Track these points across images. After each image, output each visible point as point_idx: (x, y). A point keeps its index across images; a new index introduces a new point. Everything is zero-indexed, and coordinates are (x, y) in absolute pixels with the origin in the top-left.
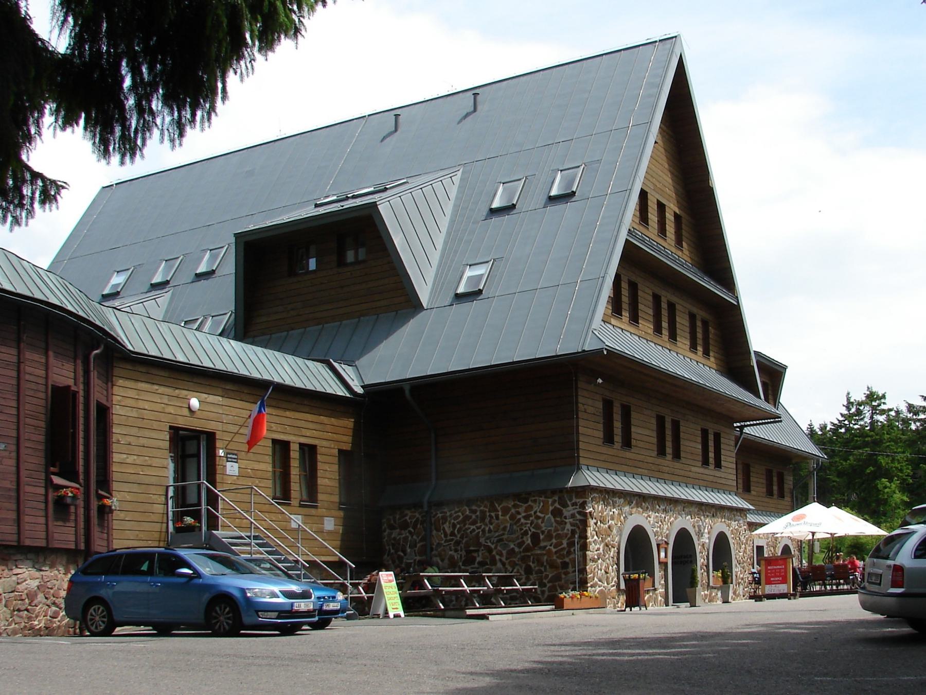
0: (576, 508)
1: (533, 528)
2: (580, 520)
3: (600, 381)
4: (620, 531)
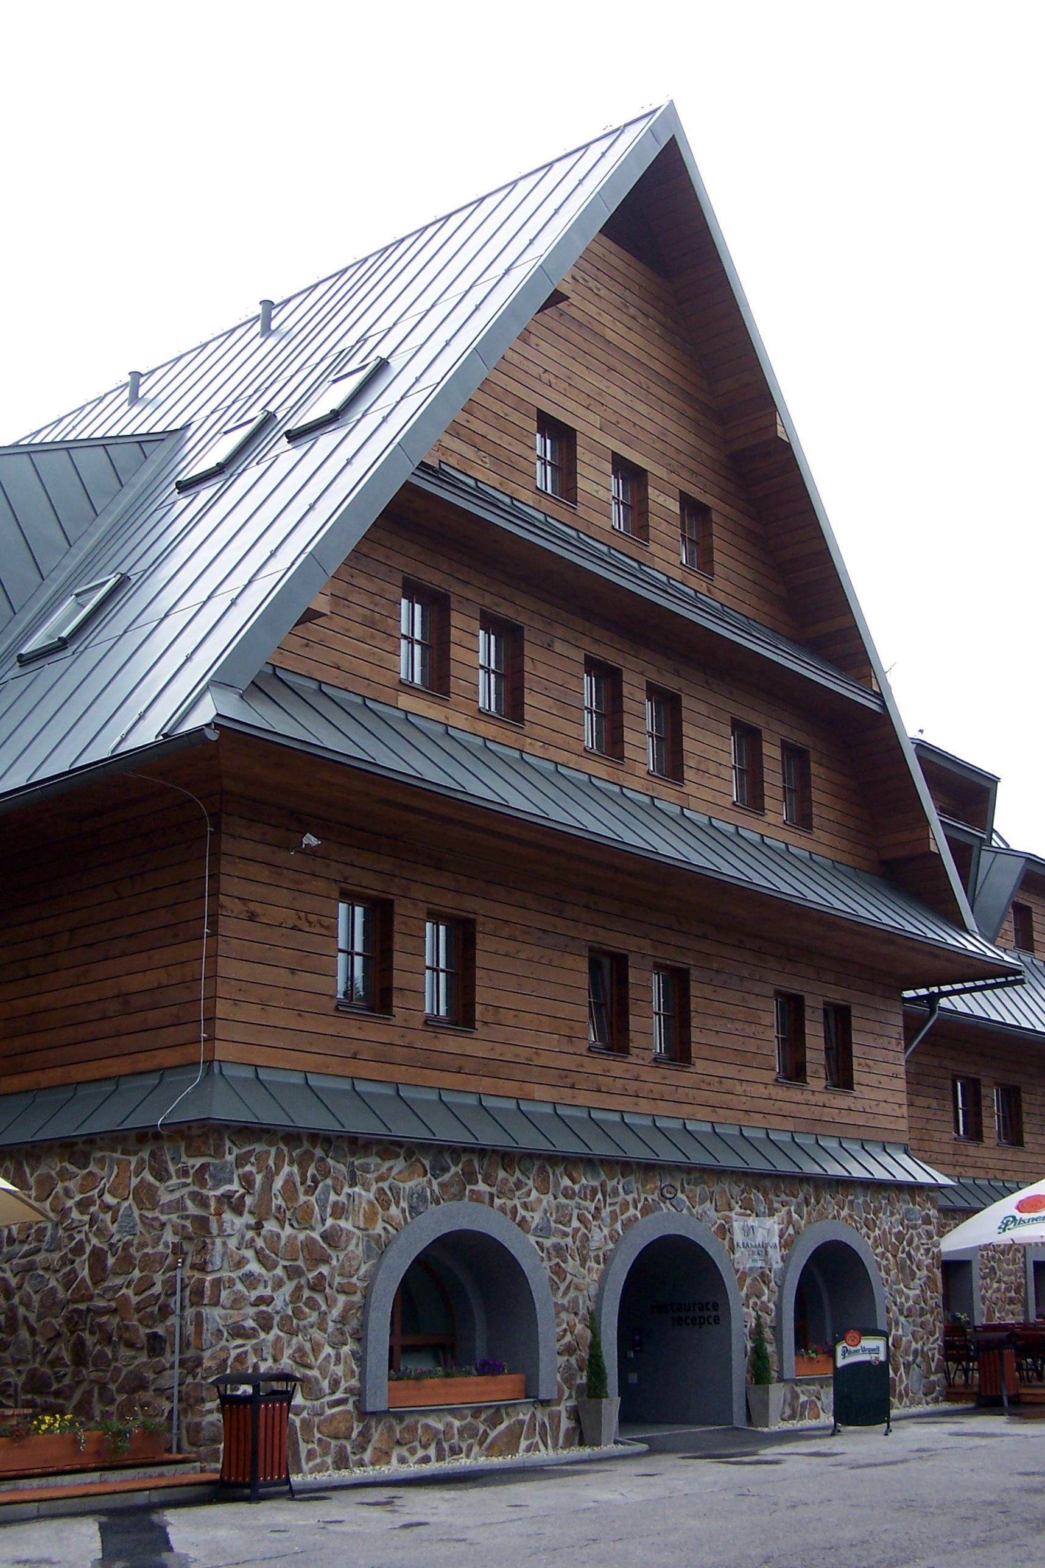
0: (186, 1185)
1: (96, 1235)
2: (196, 1219)
3: (310, 840)
4: (379, 1248)
